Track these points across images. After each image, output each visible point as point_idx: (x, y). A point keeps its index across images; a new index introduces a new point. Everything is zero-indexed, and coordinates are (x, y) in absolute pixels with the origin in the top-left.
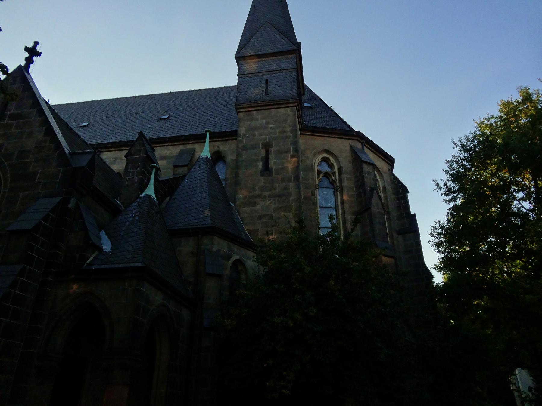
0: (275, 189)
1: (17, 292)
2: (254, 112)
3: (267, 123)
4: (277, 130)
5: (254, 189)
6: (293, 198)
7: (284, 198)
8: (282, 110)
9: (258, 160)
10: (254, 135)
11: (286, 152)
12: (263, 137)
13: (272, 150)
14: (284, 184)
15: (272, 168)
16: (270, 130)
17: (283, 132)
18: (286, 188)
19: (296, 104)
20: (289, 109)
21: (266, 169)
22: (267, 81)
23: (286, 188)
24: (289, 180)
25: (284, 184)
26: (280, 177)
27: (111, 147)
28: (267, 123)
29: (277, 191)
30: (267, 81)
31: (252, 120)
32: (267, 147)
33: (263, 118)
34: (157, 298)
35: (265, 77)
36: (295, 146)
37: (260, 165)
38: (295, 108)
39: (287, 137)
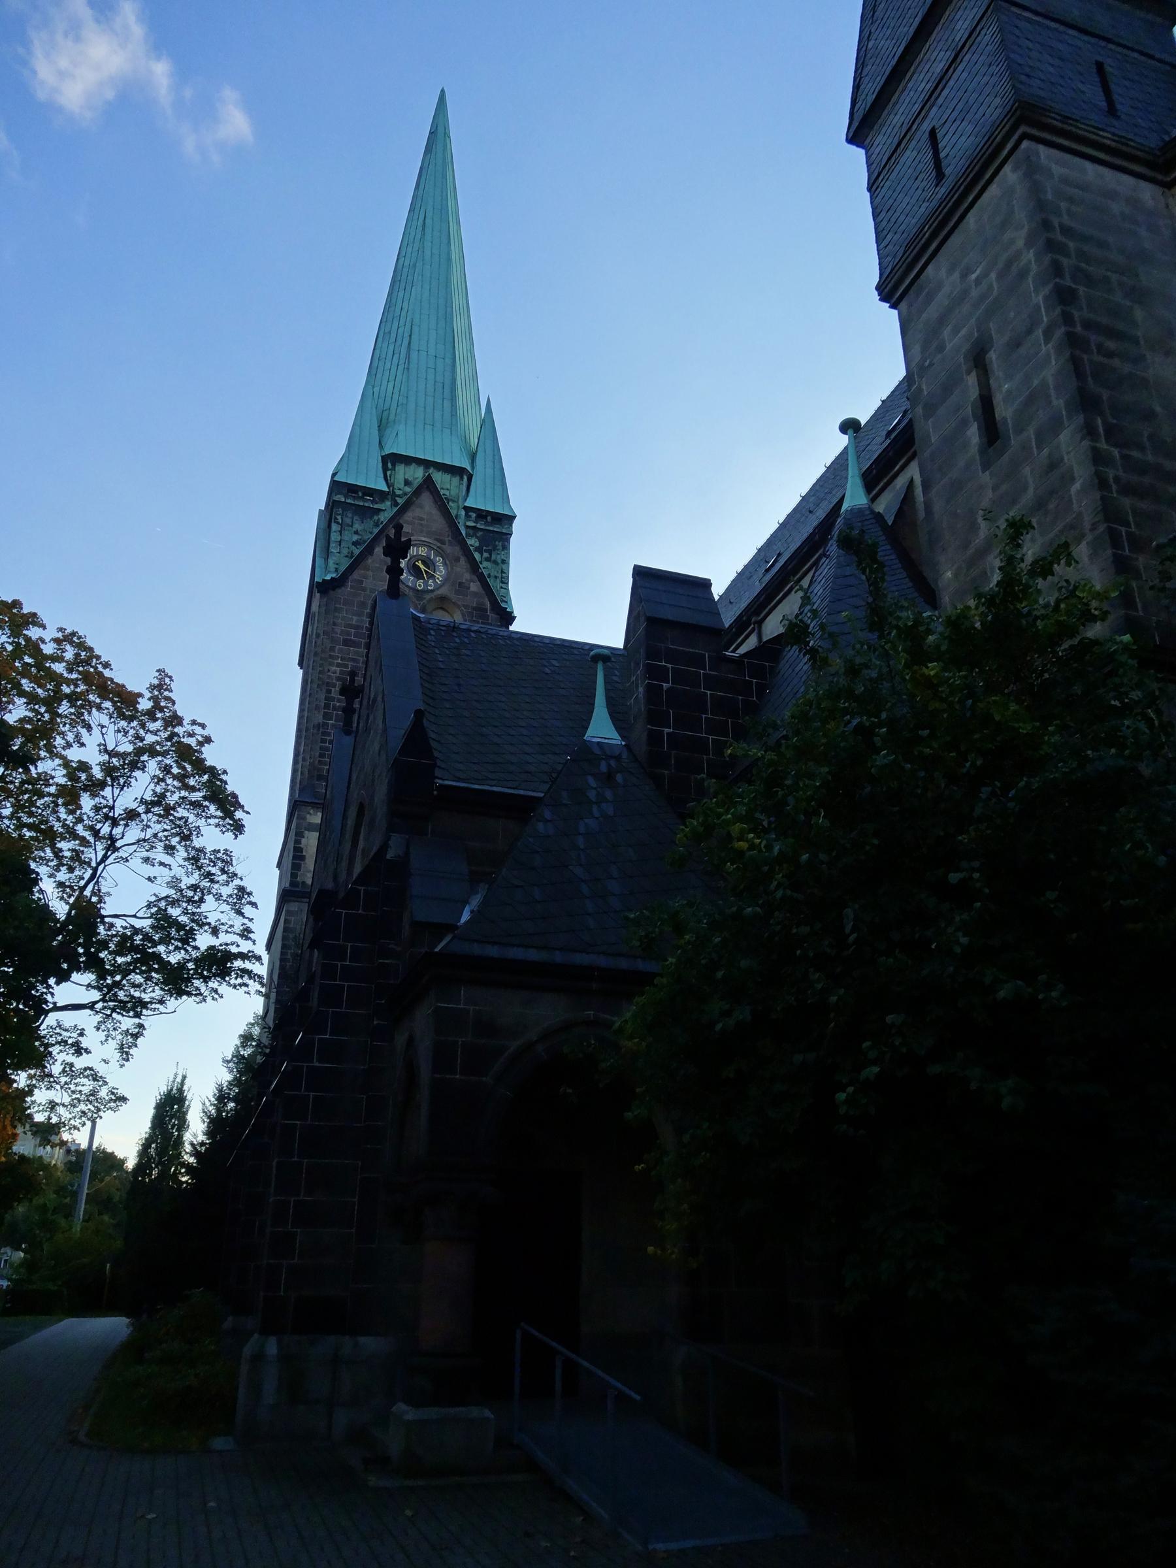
0: (1025, 489)
1: (317, 1064)
2: (930, 269)
3: (964, 275)
4: (993, 276)
5: (973, 527)
6: (1077, 486)
7: (1051, 506)
8: (993, 190)
9: (964, 423)
10: (941, 348)
11: (1030, 331)
12: (963, 332)
13: (992, 356)
14: (1046, 451)
15: (1005, 419)
16: (975, 293)
17: (1009, 264)
18: (1053, 465)
19: (1023, 129)
20: (1007, 168)
21: (992, 432)
22: (933, 133)
23: (1053, 465)
24: (1055, 426)
25: (1046, 451)
26: (1031, 432)
27: (770, 598)
28: (964, 275)
29: (1031, 491)
30: (933, 133)
31: (930, 298)
32: (978, 359)
33: (951, 271)
34: (540, 1014)
35: (926, 126)
36: (1050, 286)
37: (973, 433)
38: (1025, 144)
39: (1023, 274)
